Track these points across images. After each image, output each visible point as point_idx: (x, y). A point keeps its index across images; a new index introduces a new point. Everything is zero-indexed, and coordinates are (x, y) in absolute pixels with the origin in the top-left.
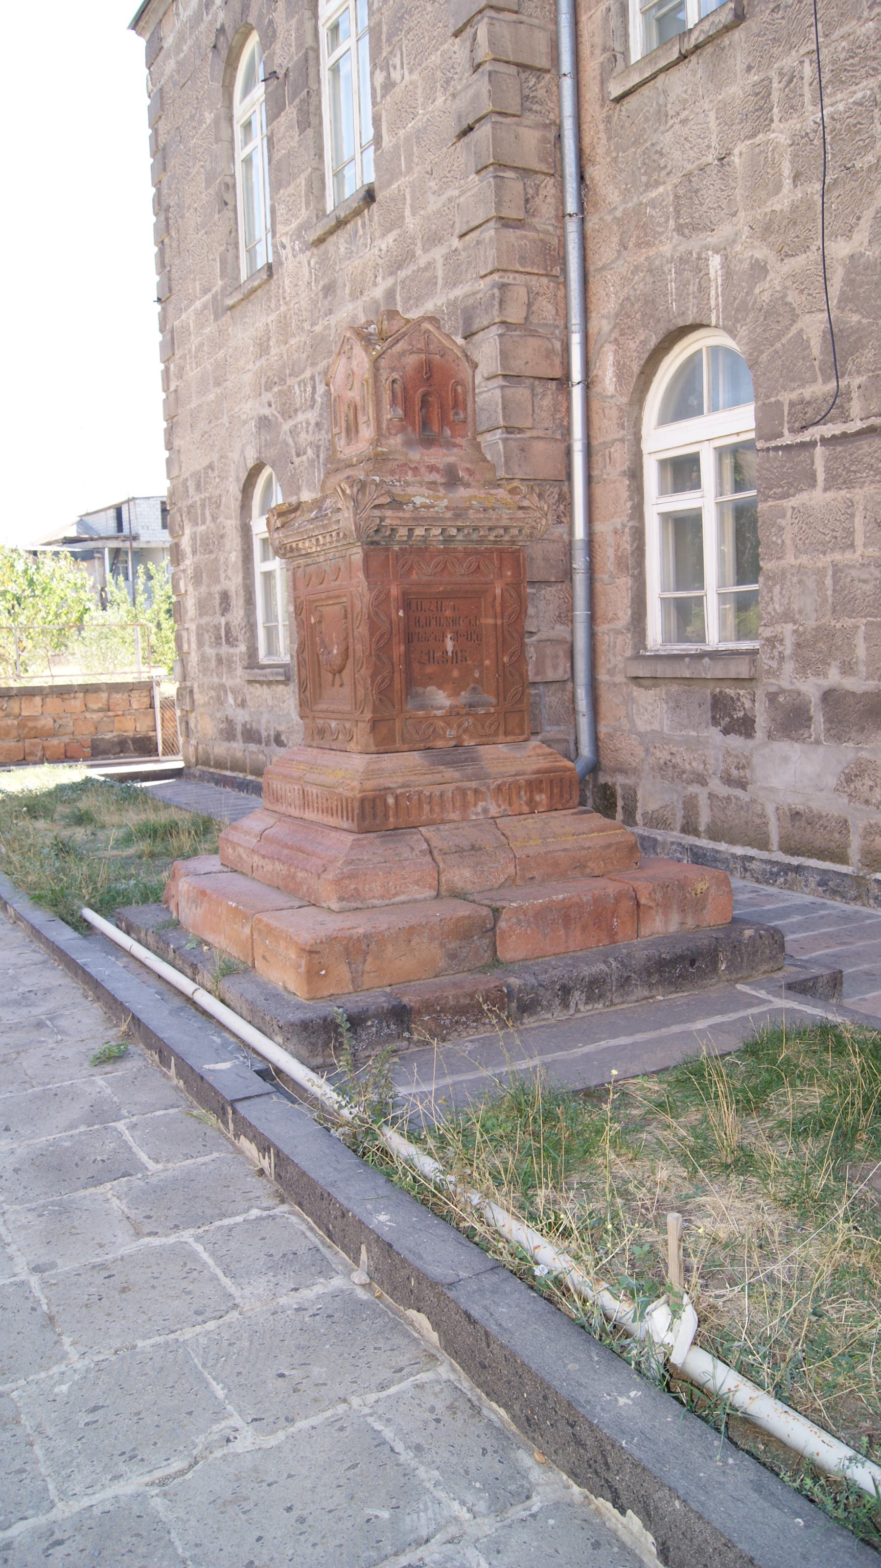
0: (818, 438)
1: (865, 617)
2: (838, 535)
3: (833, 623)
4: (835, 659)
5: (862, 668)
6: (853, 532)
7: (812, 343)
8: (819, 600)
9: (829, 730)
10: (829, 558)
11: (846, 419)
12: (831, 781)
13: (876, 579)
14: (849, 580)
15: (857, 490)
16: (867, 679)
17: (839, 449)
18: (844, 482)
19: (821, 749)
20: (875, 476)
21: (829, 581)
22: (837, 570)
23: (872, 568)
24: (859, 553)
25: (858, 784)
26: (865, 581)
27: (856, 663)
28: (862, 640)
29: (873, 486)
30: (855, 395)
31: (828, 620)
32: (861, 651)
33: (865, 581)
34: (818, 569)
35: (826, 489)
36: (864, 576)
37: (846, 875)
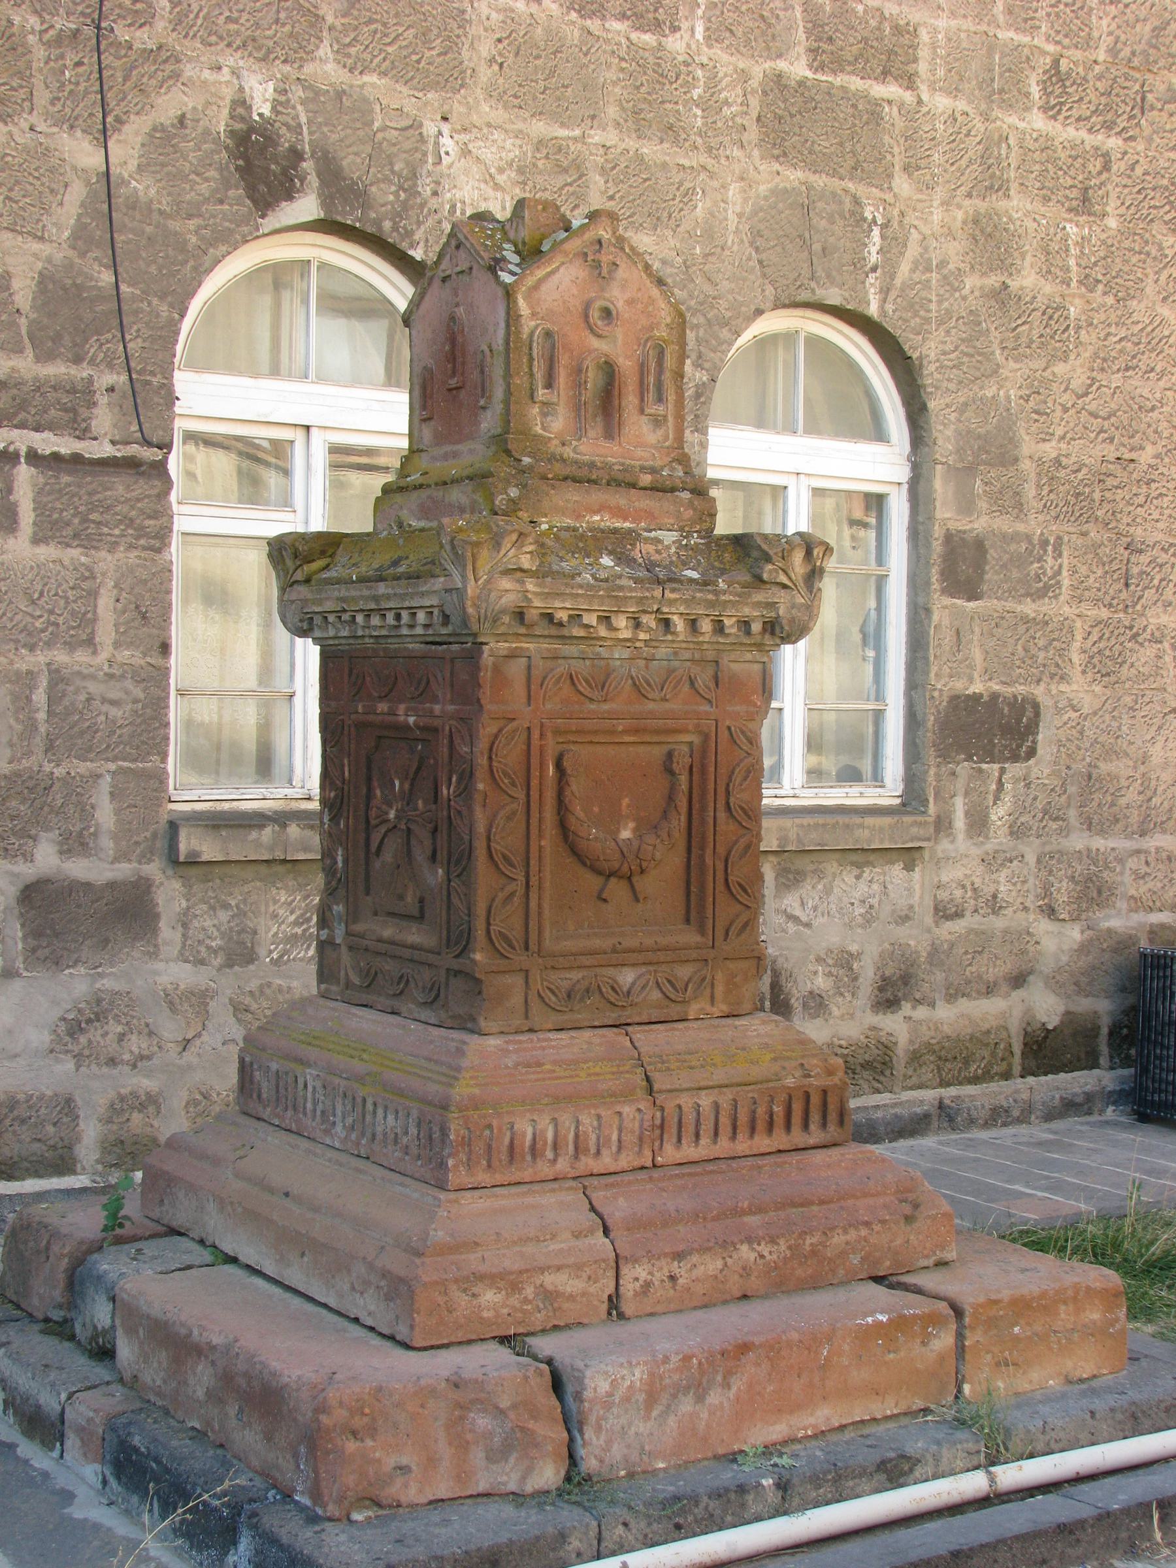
0: (23, 450)
1: (115, 759)
2: (61, 620)
3: (48, 768)
4: (48, 829)
5: (107, 844)
6: (95, 620)
7: (16, 284)
8: (19, 728)
9: (34, 950)
10: (41, 658)
11: (84, 434)
12: (40, 1038)
13: (136, 701)
14: (82, 697)
15: (103, 554)
16: (116, 860)
17: (66, 479)
18: (76, 536)
19: (17, 985)
20: (138, 538)
21: (40, 697)
22: (58, 678)
23: (129, 684)
24: (104, 656)
25: (94, 1034)
26: (114, 703)
27: (95, 835)
28: (106, 799)
29: (133, 554)
30: (103, 399)
31: (37, 761)
32: (105, 815)
33: (114, 703)
34: (18, 673)
35: (36, 541)
36: (113, 695)
37: (84, 1190)
